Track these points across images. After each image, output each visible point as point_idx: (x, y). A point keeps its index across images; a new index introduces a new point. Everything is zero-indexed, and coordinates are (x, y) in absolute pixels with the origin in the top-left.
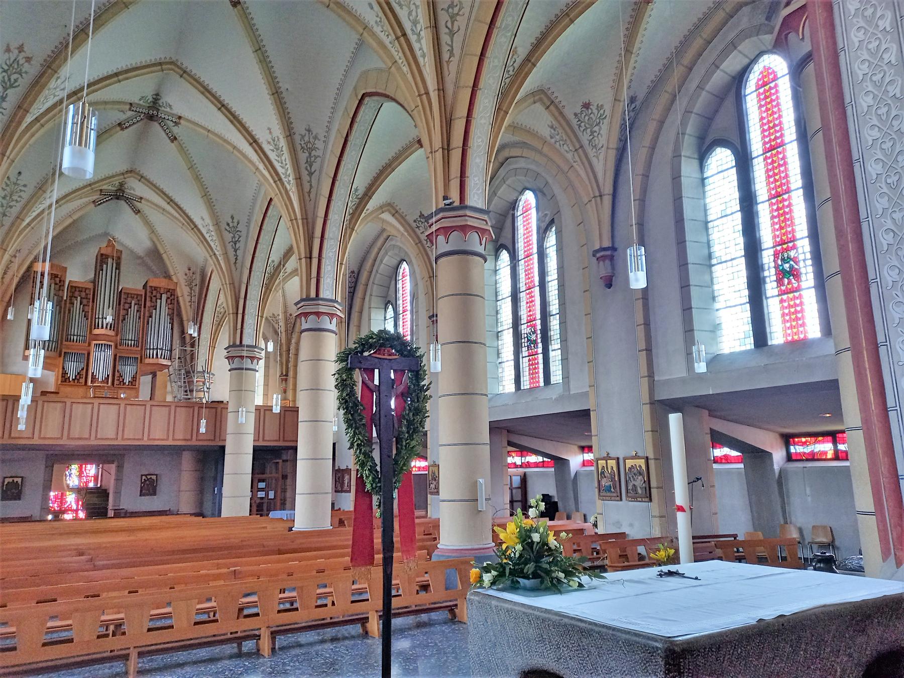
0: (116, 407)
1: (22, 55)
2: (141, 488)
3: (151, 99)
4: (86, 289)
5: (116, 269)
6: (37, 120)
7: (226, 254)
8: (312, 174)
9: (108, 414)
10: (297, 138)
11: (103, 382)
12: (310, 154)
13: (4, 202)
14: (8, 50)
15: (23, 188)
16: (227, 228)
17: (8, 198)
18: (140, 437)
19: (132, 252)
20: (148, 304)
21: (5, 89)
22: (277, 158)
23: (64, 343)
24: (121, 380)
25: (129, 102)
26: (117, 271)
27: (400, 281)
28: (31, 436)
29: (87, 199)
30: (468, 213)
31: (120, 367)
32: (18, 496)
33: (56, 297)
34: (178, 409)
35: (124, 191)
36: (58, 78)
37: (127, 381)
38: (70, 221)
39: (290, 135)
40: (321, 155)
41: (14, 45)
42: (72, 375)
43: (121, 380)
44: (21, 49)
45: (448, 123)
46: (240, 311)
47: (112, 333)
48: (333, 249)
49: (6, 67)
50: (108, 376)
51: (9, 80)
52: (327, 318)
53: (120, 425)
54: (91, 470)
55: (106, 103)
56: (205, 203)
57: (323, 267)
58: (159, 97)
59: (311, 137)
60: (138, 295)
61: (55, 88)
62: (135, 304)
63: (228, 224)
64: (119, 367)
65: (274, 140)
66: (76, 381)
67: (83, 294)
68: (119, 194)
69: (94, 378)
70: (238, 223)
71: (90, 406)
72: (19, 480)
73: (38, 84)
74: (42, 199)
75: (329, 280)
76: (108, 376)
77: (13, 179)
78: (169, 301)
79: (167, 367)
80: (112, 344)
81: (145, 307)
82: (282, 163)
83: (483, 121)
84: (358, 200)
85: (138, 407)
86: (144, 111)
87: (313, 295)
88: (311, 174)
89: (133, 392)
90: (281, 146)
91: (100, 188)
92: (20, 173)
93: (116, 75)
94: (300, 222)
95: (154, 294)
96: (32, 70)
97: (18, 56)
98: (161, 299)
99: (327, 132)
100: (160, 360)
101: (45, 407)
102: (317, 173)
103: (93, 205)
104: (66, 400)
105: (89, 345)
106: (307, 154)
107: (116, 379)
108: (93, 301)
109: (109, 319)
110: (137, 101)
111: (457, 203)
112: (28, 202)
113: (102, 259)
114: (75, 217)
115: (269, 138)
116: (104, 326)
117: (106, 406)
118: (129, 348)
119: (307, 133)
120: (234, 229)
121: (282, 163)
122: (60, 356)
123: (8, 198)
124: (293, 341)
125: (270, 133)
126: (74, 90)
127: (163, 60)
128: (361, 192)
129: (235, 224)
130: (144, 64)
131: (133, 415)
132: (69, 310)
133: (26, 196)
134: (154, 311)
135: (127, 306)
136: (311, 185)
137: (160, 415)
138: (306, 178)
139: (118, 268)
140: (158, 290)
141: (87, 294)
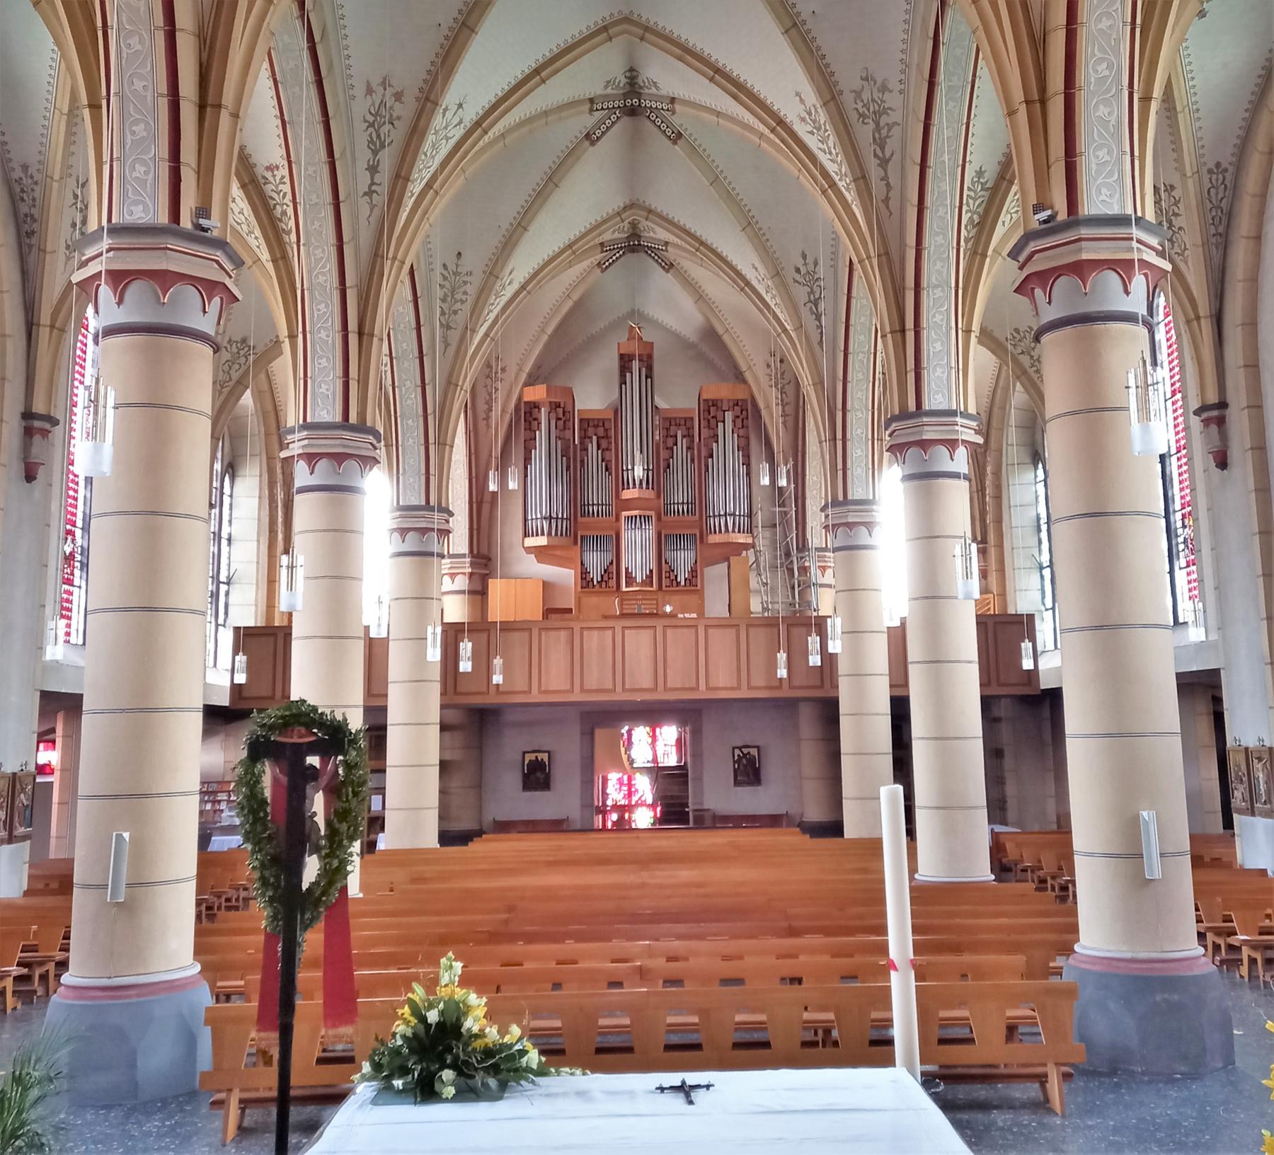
0: (650, 632)
1: (389, 91)
2: (735, 771)
3: (624, 81)
4: (604, 421)
5: (647, 378)
6: (429, 186)
7: (799, 327)
8: (887, 161)
9: (639, 643)
10: (848, 99)
11: (643, 583)
12: (877, 124)
13: (445, 306)
14: (370, 91)
15: (465, 279)
16: (797, 277)
17: (449, 299)
18: (694, 685)
19: (677, 336)
20: (705, 433)
21: (375, 153)
22: (820, 145)
24: (673, 577)
25: (587, 96)
26: (649, 380)
27: (1162, 326)
28: (526, 689)
29: (586, 264)
30: (1085, 232)
31: (668, 553)
32: (545, 785)
33: (559, 442)
34: (751, 630)
35: (640, 236)
36: (445, 110)
37: (681, 579)
38: (570, 303)
39: (833, 98)
40: (900, 121)
41: (375, 82)
42: (595, 575)
43: (673, 577)
44: (385, 83)
45: (1039, 44)
46: (839, 435)
47: (650, 494)
48: (942, 306)
49: (371, 119)
50: (651, 571)
51: (379, 136)
52: (943, 451)
53: (659, 662)
54: (669, 733)
55: (546, 113)
56: (750, 240)
57: (924, 346)
58: (635, 73)
59: (875, 91)
60: (686, 419)
61: (446, 128)
62: (684, 436)
63: (798, 270)
64: (668, 555)
65: (810, 114)
66: (604, 584)
67: (601, 431)
68: (634, 244)
69: (630, 580)
70: (816, 264)
71: (609, 633)
72: (545, 757)
73: (416, 133)
74: (497, 287)
75: (939, 370)
77: (452, 267)
78: (739, 422)
79: (746, 547)
80: (652, 513)
82: (830, 153)
83: (1105, 24)
84: (986, 194)
85: (685, 630)
86: (617, 104)
87: (912, 406)
88: (884, 163)
89: (692, 599)
90: (822, 122)
91: (600, 239)
92: (459, 254)
93: (537, 71)
94: (875, 262)
96: (405, 111)
97: (384, 95)
98: (724, 422)
99: (903, 72)
100: (732, 535)
101: (543, 637)
102: (897, 157)
103: (599, 271)
104: (572, 624)
106: (872, 125)
107: (663, 576)
109: (639, 472)
110: (600, 91)
111: (1062, 216)
112: (478, 298)
113: (625, 362)
114: (575, 297)
115: (800, 110)
116: (637, 482)
117: (633, 631)
119: (865, 83)
120: (811, 279)
121: (830, 153)
122: (576, 543)
123: (449, 299)
124: (989, 469)
125: (802, 101)
126: (475, 119)
127: (608, 20)
128: (990, 176)
129: (811, 267)
130: (578, 37)
131: (678, 642)
132: (582, 461)
133: (471, 290)
134: (714, 444)
135: (670, 442)
136: (888, 185)
137: (722, 642)
138: (874, 172)
139: (649, 376)
140: (719, 405)
141: (606, 430)
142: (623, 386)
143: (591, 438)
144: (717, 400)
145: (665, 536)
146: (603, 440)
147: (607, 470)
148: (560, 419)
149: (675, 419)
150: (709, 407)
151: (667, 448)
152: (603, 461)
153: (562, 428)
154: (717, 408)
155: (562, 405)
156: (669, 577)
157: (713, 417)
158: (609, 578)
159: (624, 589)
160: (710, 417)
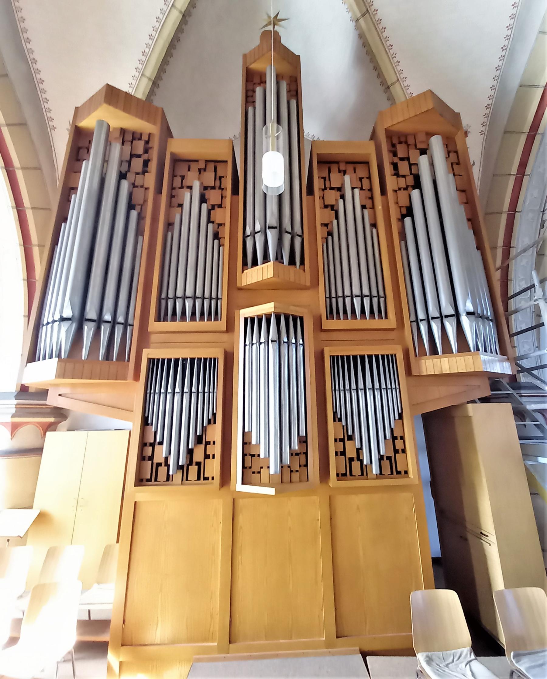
20: (391, 182)
23: (154, 326)
50: (303, 441)
67: (209, 178)
76: (303, 441)
81: (383, 192)
95: (400, 155)
105: (230, 327)
108: (235, 191)
118: (359, 323)
132: (169, 225)
140: (411, 141)
142: (251, 110)
143: (190, 188)
144: (406, 136)
145: (332, 357)
146: (213, 191)
147: (216, 236)
148: (139, 156)
149: (337, 163)
150: (394, 146)
151: (326, 207)
152: (209, 221)
153: (140, 169)
154: (408, 146)
155: (145, 137)
156: (343, 453)
157: (402, 159)
158: (207, 457)
159: (240, 487)
160: (396, 160)
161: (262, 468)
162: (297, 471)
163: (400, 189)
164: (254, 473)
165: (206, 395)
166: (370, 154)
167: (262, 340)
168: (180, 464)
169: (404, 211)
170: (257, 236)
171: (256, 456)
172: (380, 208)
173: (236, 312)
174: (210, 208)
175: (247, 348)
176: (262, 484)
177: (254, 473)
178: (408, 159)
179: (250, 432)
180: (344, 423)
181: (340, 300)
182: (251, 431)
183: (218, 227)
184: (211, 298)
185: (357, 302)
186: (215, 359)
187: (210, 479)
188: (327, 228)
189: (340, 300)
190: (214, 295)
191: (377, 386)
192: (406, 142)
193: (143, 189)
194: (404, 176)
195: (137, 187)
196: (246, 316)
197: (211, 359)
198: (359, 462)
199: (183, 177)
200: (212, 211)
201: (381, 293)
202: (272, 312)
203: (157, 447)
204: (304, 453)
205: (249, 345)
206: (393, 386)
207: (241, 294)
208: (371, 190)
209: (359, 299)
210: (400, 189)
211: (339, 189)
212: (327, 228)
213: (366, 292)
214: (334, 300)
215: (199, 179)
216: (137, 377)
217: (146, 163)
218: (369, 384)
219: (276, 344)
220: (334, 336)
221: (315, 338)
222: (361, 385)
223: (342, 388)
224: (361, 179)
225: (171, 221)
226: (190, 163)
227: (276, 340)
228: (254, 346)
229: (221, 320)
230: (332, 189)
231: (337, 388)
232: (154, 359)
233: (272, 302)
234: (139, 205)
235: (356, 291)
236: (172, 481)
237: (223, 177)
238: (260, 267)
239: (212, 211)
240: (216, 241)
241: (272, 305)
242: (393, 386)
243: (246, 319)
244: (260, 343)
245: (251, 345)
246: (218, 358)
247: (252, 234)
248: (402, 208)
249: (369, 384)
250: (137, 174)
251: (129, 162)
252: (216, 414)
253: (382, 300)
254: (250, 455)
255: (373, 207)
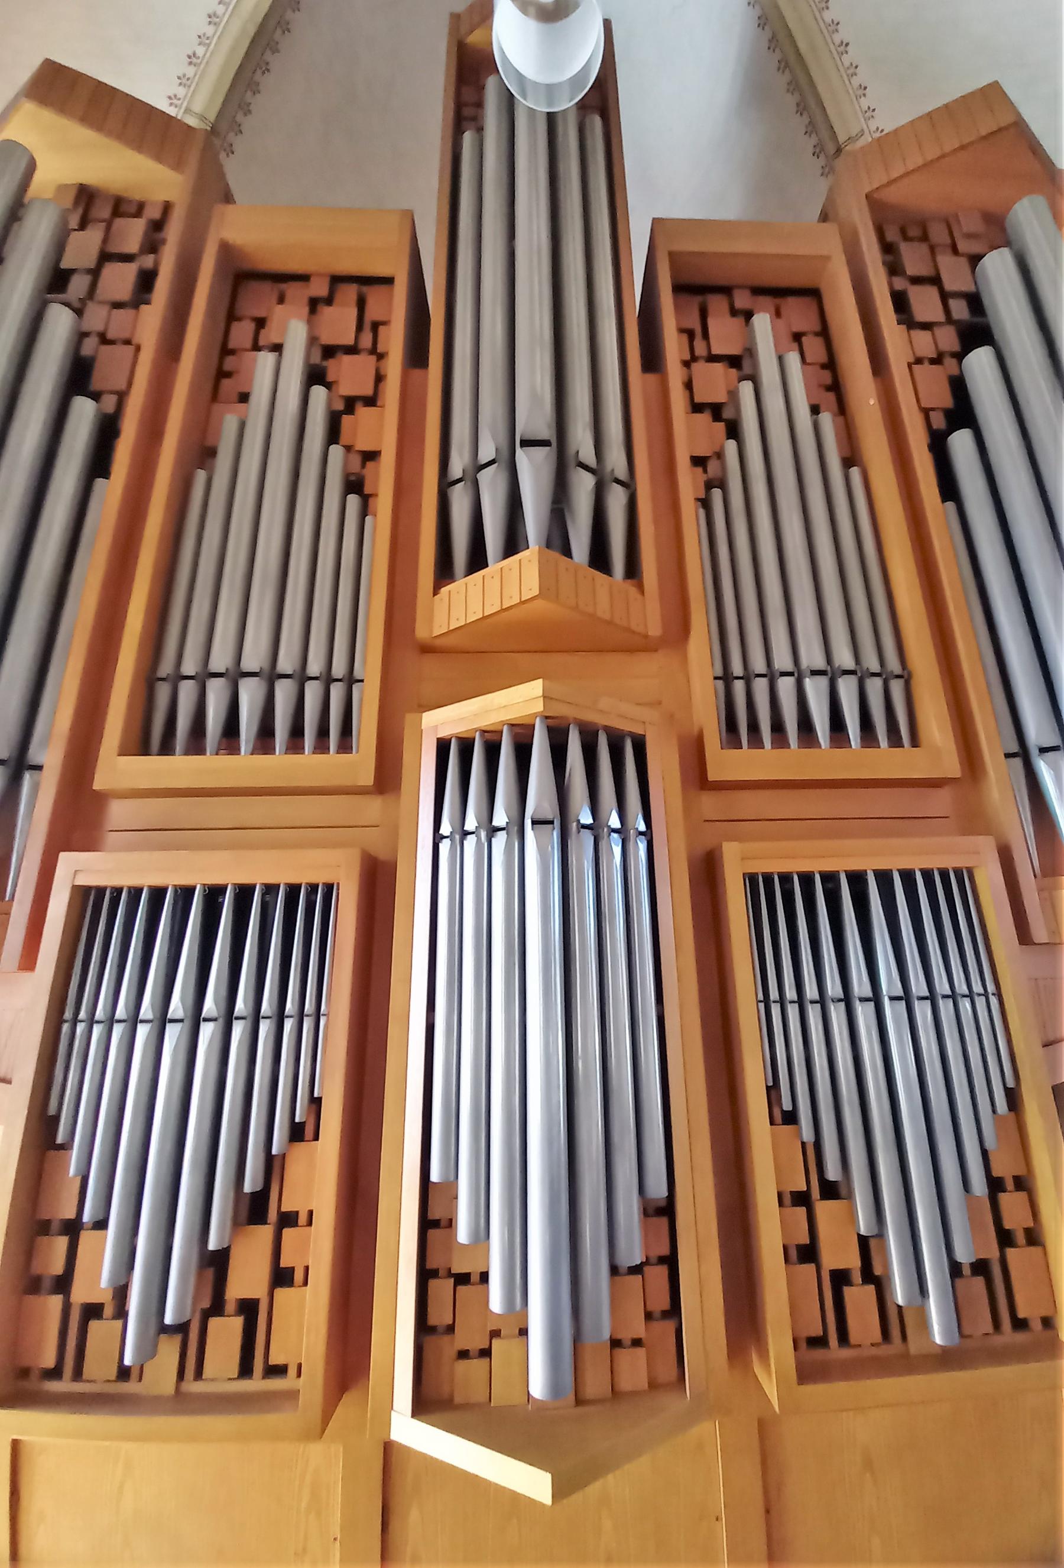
95: (911, 271)
140: (938, 234)
145: (751, 879)
146: (347, 359)
147: (354, 485)
148: (127, 258)
149: (726, 291)
151: (697, 408)
154: (932, 249)
156: (808, 1253)
157: (916, 280)
158: (282, 1277)
160: (900, 284)
161: (495, 1334)
162: (637, 1343)
163: (919, 361)
164: (463, 1354)
165: (289, 1025)
166: (827, 258)
167: (500, 818)
168: (168, 1320)
169: (939, 422)
170: (485, 477)
171: (475, 1278)
172: (872, 402)
173: (409, 717)
174: (340, 406)
175: (445, 847)
176: (495, 1407)
177: (463, 1354)
178: (936, 281)
179: (450, 1188)
180: (807, 1133)
181: (761, 687)
182: (452, 1178)
183: (363, 466)
184: (328, 679)
185: (816, 692)
186: (329, 888)
187: (292, 1371)
188: (705, 471)
189: (761, 687)
190: (339, 669)
191: (918, 986)
192: (924, 238)
193: (130, 349)
194: (927, 326)
195: (111, 342)
196: (443, 733)
197: (313, 888)
198: (871, 1288)
199: (261, 323)
200: (346, 419)
201: (893, 664)
202: (535, 715)
203: (86, 1238)
204: (662, 1260)
205: (450, 837)
206: (977, 988)
207: (430, 665)
208: (831, 364)
209: (823, 682)
210: (919, 361)
211: (734, 361)
212: (705, 471)
213: (844, 658)
214: (739, 686)
215: (310, 322)
216: (29, 960)
217: (146, 281)
218: (889, 981)
219: (553, 834)
220: (749, 803)
221: (688, 809)
222: (860, 985)
223: (791, 993)
224: (797, 337)
225: (209, 443)
226: (283, 286)
227: (550, 817)
228: (470, 842)
229: (357, 752)
230: (712, 358)
231: (774, 994)
232: (100, 891)
233: (539, 678)
234: (112, 392)
235: (812, 656)
236: (140, 1380)
237: (384, 323)
238: (495, 566)
239: (346, 419)
240: (353, 500)
241: (535, 688)
242: (977, 988)
243: (443, 747)
244: (494, 830)
245: (457, 837)
246: (338, 884)
247: (470, 473)
248: (931, 413)
249: (889, 981)
250: (117, 305)
251: (95, 273)
252: (319, 1099)
253: (897, 689)
254: (450, 1274)
255: (842, 409)
